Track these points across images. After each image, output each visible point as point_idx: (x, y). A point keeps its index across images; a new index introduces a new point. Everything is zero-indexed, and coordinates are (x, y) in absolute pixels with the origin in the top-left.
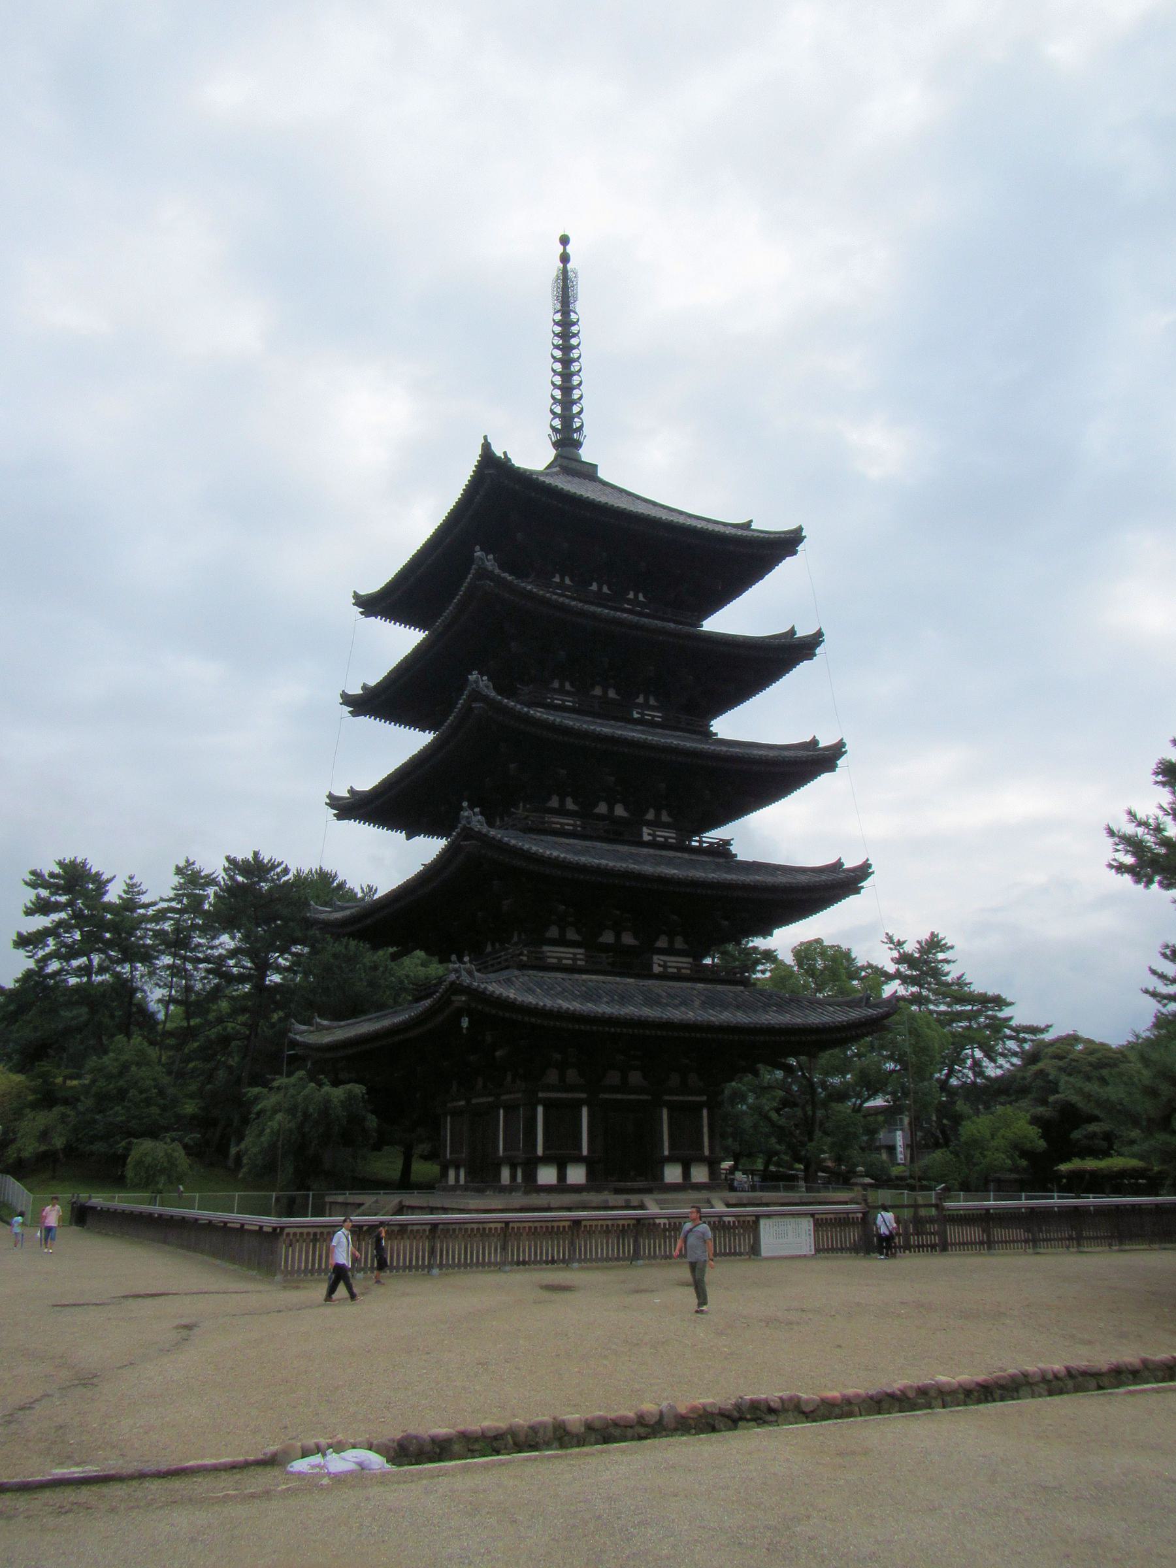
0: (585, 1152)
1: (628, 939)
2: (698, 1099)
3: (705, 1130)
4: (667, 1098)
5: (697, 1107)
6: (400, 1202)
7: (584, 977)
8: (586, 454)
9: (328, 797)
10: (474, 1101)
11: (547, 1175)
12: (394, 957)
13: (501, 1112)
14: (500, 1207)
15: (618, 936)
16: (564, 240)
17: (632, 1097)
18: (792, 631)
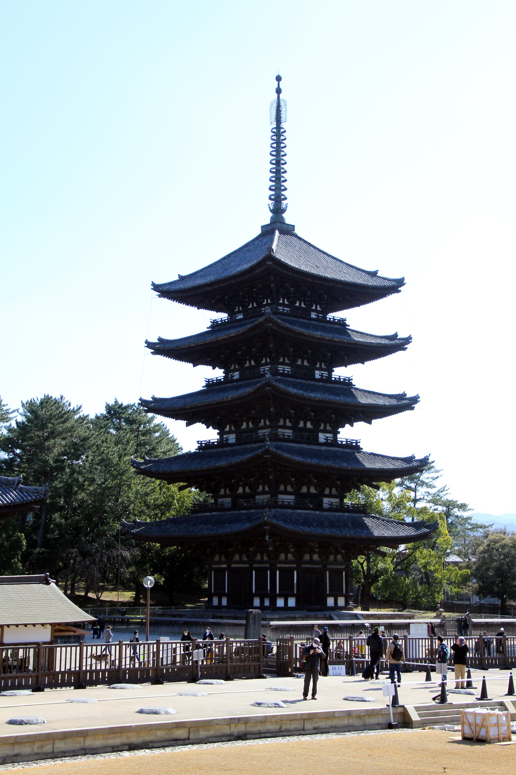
0: (295, 592)
1: (313, 490)
2: (339, 567)
3: (344, 582)
4: (328, 566)
5: (340, 571)
6: (214, 614)
7: (299, 511)
8: (288, 218)
9: (140, 400)
10: (233, 566)
11: (280, 603)
12: (181, 489)
13: (254, 572)
14: (278, 617)
15: (308, 489)
16: (279, 79)
17: (314, 566)
18: (396, 335)
